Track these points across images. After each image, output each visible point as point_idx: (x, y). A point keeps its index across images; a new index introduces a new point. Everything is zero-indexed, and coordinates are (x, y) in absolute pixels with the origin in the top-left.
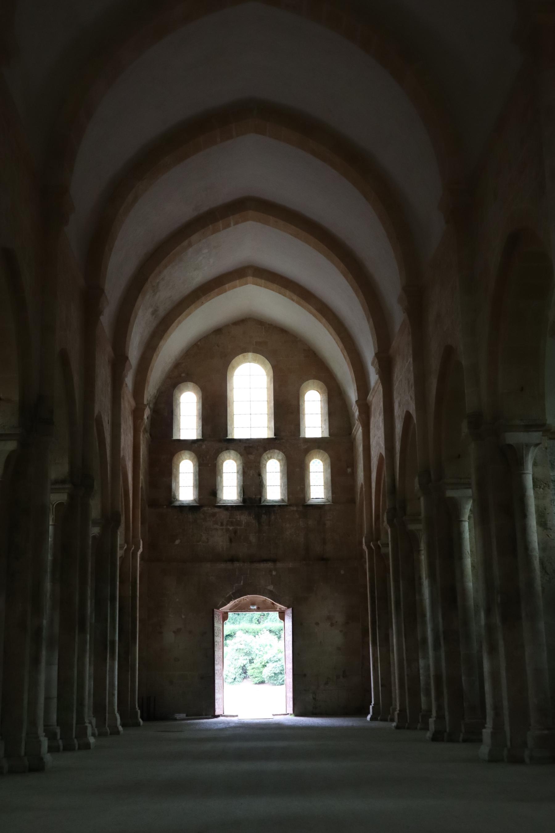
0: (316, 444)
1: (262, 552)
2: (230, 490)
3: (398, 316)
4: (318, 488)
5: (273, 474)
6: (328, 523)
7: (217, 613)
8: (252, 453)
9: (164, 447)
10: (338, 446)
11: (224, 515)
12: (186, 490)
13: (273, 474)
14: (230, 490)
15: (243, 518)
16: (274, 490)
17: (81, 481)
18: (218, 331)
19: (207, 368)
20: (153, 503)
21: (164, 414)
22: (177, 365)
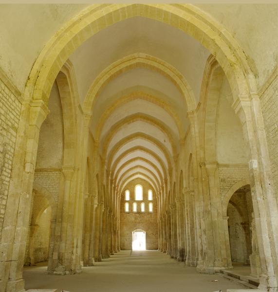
0: (151, 201)
1: (141, 220)
2: (135, 210)
3: (167, 172)
4: (151, 209)
5: (143, 206)
6: (152, 216)
7: (133, 232)
8: (139, 203)
9: (123, 201)
10: (155, 202)
11: (134, 214)
12: (127, 210)
13: (143, 206)
14: (135, 210)
15: (137, 215)
16: (143, 210)
17: (114, 215)
18: (133, 180)
19: (131, 187)
20: (121, 212)
21: (123, 196)
22: (125, 187)
